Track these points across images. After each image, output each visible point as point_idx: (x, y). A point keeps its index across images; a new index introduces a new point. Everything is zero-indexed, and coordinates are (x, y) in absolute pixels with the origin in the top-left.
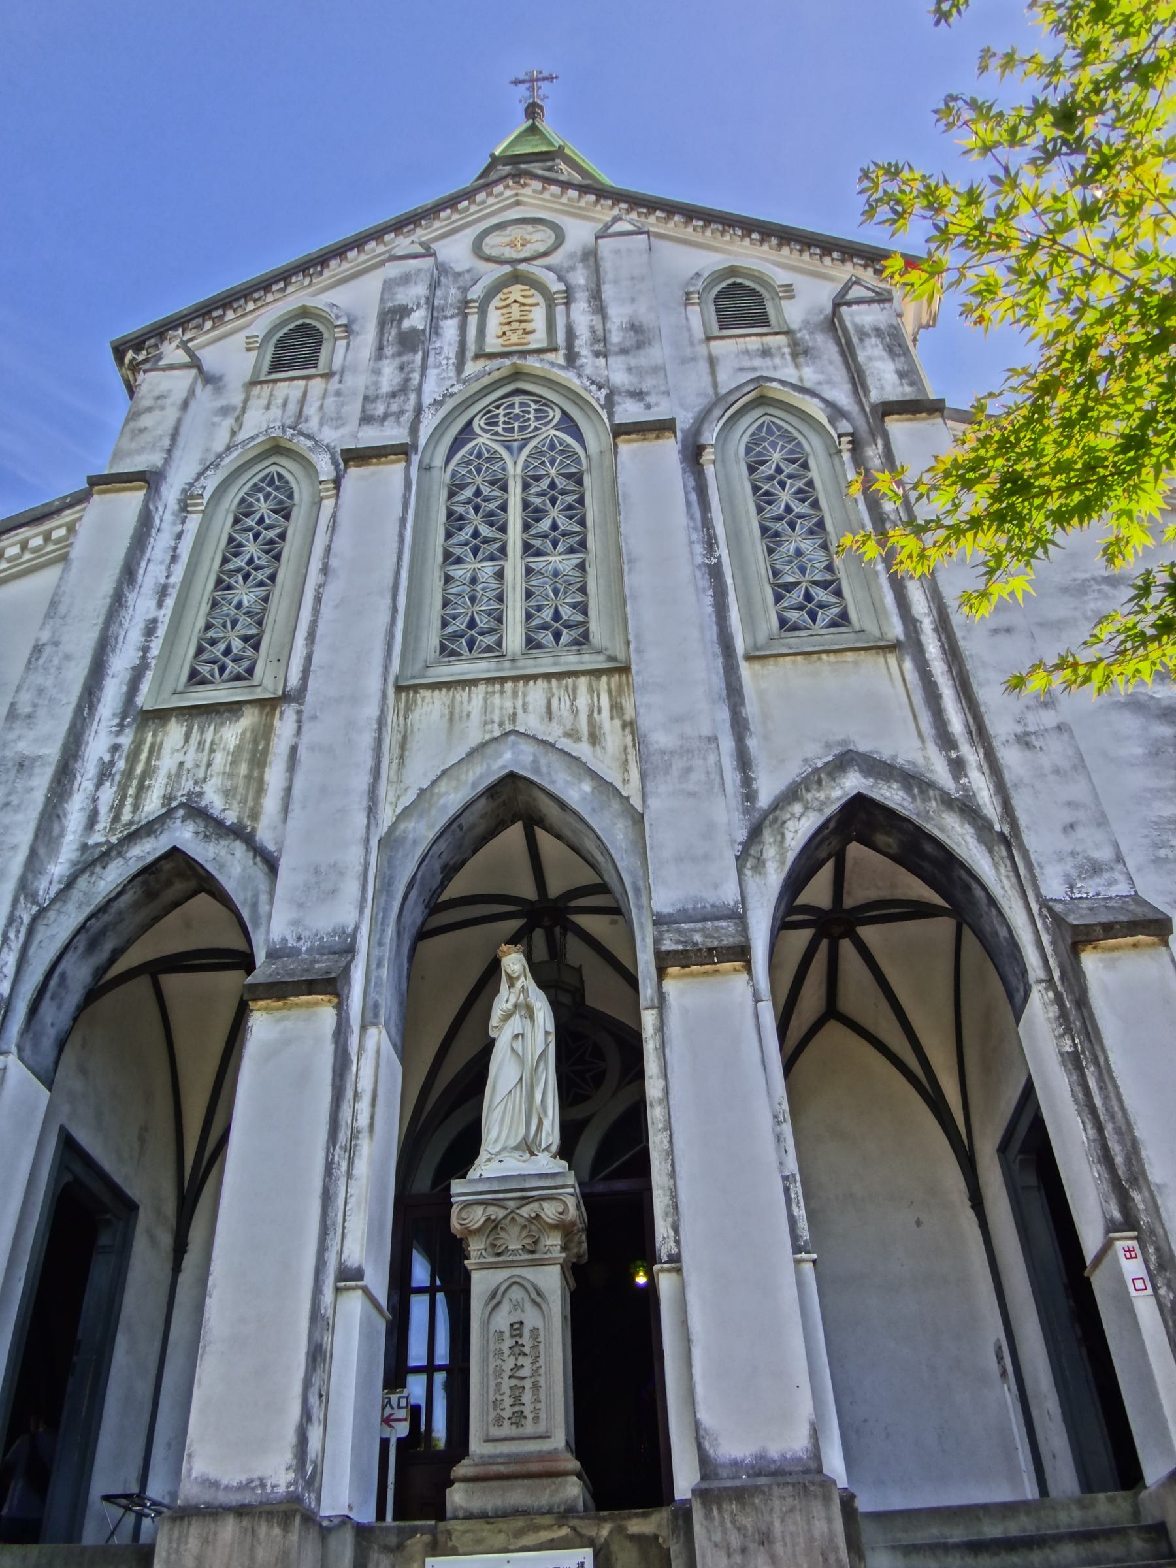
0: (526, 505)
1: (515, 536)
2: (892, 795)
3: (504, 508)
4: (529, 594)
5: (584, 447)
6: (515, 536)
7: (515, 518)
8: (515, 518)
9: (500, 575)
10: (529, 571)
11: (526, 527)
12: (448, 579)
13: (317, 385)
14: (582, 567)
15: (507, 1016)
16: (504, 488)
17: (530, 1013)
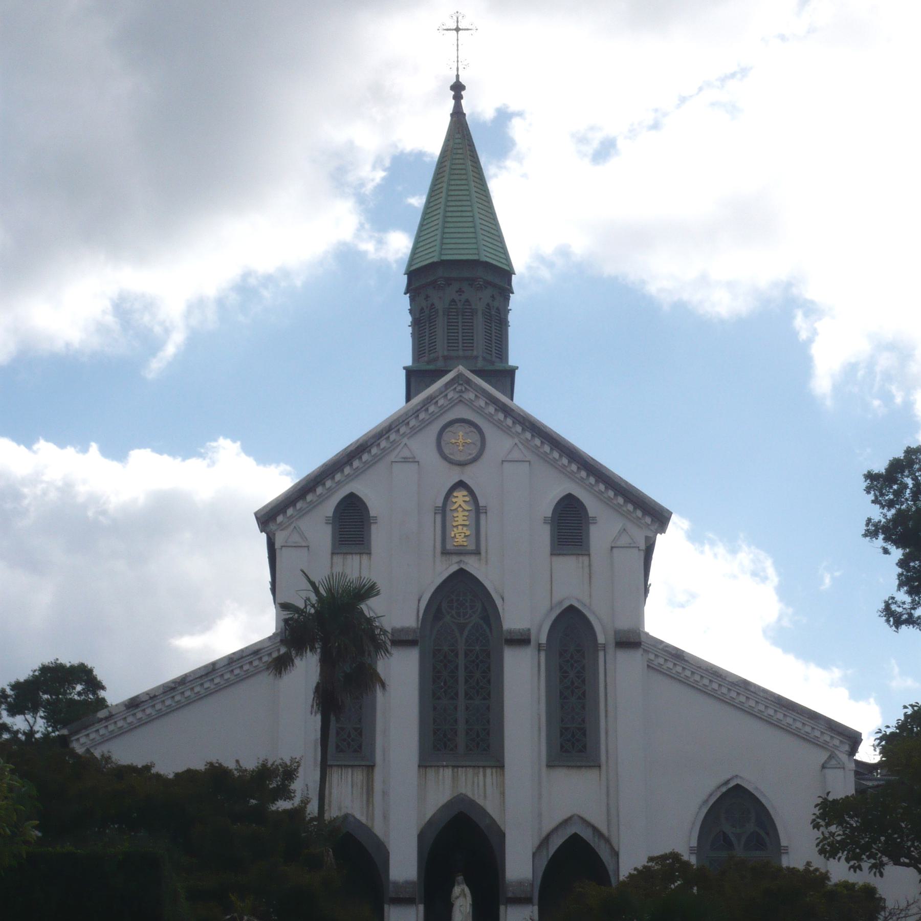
0: (466, 668)
1: (462, 689)
2: (586, 835)
3: (457, 667)
4: (467, 722)
5: (491, 629)
6: (462, 689)
7: (461, 674)
8: (461, 674)
9: (456, 708)
10: (467, 708)
11: (466, 681)
12: (435, 709)
13: (365, 557)
14: (488, 708)
15: (457, 898)
16: (457, 655)
17: (465, 896)
